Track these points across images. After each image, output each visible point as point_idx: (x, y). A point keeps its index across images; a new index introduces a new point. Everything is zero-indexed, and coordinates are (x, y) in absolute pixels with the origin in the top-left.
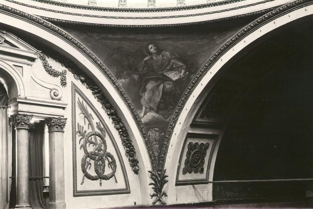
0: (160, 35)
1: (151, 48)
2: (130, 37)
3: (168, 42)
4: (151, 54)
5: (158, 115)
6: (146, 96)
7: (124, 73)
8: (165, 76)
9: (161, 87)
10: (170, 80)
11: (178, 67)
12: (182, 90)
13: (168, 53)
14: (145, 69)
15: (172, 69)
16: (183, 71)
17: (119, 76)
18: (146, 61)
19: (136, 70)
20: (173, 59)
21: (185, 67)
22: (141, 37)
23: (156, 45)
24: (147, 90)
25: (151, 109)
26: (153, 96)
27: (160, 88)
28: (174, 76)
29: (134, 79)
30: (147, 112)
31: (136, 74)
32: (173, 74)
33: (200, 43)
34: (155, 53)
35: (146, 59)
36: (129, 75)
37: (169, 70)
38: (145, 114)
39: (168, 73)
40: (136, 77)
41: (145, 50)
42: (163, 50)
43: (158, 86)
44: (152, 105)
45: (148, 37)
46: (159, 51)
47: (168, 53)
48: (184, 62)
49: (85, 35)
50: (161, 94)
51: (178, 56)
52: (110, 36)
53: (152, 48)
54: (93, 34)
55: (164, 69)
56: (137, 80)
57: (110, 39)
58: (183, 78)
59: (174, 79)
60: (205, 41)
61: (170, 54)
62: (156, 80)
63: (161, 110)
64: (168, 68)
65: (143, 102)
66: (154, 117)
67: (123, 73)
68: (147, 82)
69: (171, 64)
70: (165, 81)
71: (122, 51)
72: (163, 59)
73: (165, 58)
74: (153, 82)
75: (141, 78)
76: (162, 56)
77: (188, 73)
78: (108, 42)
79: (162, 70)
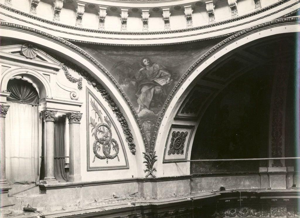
0: (151, 52)
1: (145, 61)
2: (129, 53)
3: (158, 57)
4: (145, 66)
5: (150, 111)
6: (141, 97)
7: (125, 80)
9: (152, 90)
10: (159, 85)
11: (165, 76)
12: (168, 93)
13: (157, 66)
15: (160, 77)
16: (169, 79)
17: (121, 82)
18: (141, 71)
19: (134, 78)
20: (161, 69)
21: (170, 76)
22: (137, 53)
24: (142, 93)
25: (145, 107)
26: (146, 97)
30: (142, 109)
33: (181, 58)
34: (148, 65)
35: (141, 69)
36: (129, 81)
37: (158, 78)
38: (140, 110)
39: (158, 80)
41: (140, 63)
42: (154, 63)
43: (150, 90)
44: (145, 104)
45: (142, 53)
46: (151, 64)
47: (157, 66)
48: (170, 72)
49: (96, 52)
50: (152, 95)
51: (165, 68)
52: (115, 53)
53: (146, 62)
54: (102, 51)
56: (134, 85)
58: (169, 84)
59: (162, 84)
60: (186, 56)
61: (159, 66)
62: (149, 85)
63: (152, 107)
64: (158, 76)
65: (139, 101)
66: (147, 113)
67: (124, 80)
68: (142, 86)
69: (160, 73)
70: (156, 86)
71: (123, 64)
72: (154, 70)
73: (155, 69)
75: (137, 83)
76: (153, 68)
77: (172, 80)
78: (113, 57)
79: (154, 78)
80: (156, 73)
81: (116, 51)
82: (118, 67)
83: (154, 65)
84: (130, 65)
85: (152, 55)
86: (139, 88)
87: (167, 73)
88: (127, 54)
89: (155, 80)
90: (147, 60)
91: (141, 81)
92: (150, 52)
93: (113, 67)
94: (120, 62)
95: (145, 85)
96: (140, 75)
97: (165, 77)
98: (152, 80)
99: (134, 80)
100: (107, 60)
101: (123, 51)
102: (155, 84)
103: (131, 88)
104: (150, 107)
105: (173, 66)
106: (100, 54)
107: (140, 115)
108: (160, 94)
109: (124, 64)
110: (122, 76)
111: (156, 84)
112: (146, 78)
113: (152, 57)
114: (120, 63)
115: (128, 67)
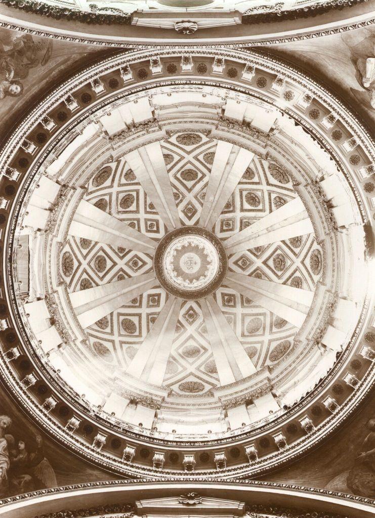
0: (19, 107)
1: (17, 88)
2: (45, 81)
3: (7, 108)
4: (12, 83)
7: (22, 43)
17: (28, 38)
18: (10, 72)
19: (12, 56)
22: (35, 90)
23: (15, 95)
29: (8, 44)
31: (9, 51)
34: (9, 87)
35: (12, 74)
36: (16, 45)
40: (7, 48)
41: (21, 81)
42: (4, 97)
45: (28, 96)
52: (62, 67)
53: (16, 89)
54: (81, 57)
56: (4, 46)
67: (24, 42)
71: (41, 61)
78: (60, 59)
81: (62, 70)
82: (44, 52)
84: (32, 67)
85: (16, 104)
88: (45, 79)
90: (15, 93)
92: (21, 105)
94: (46, 61)
96: (7, 66)
99: (10, 53)
100: (66, 51)
101: (55, 77)
106: (81, 51)
110: (31, 44)
113: (12, 102)
114: (46, 60)
115: (33, 63)
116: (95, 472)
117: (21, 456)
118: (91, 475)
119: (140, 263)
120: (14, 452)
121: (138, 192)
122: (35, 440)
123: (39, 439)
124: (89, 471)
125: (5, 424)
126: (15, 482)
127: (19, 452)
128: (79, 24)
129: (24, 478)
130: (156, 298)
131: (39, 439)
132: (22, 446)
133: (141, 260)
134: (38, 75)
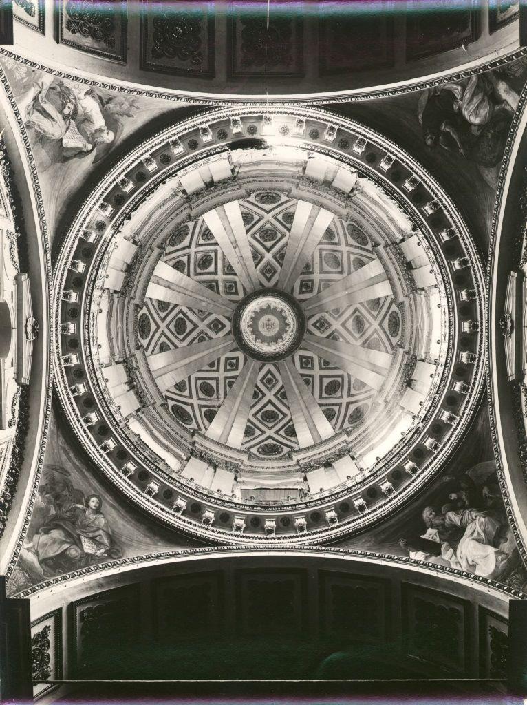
1: (93, 501)
2: (86, 473)
3: (113, 511)
4: (88, 506)
5: (39, 565)
6: (43, 538)
7: (47, 496)
8: (79, 540)
9: (66, 546)
10: (82, 548)
12: (87, 564)
13: (103, 521)
14: (68, 514)
15: (93, 539)
16: (103, 551)
17: (42, 490)
18: (76, 508)
19: (60, 506)
21: (107, 548)
22: (94, 483)
23: (100, 503)
25: (37, 553)
27: (63, 546)
28: (88, 547)
29: (48, 510)
31: (55, 509)
32: (89, 545)
33: (141, 538)
34: (92, 509)
36: (50, 502)
38: (28, 549)
40: (53, 511)
42: (101, 513)
43: (63, 542)
44: (40, 551)
46: (98, 511)
47: (103, 521)
49: (55, 431)
50: (59, 552)
52: (72, 455)
53: (93, 502)
55: (84, 532)
57: (70, 459)
59: (86, 551)
61: (105, 523)
62: (68, 535)
63: (46, 564)
64: (90, 534)
65: (36, 537)
66: (33, 563)
67: (47, 493)
68: (57, 527)
69: (97, 533)
70: (77, 545)
72: (93, 522)
73: (97, 522)
74: (63, 534)
75: (56, 517)
76: (96, 519)
78: (64, 457)
80: (92, 529)
81: (74, 455)
82: (56, 474)
83: (100, 516)
84: (72, 486)
86: (52, 525)
87: (106, 541)
89: (82, 537)
90: (97, 503)
91: (63, 519)
93: (52, 466)
95: (64, 529)
96: (70, 511)
97: (99, 544)
98: (78, 532)
99: (57, 508)
102: (77, 541)
103: (41, 512)
104: (43, 562)
105: (123, 539)
106: (55, 436)
107: (23, 552)
108: (73, 559)
109: (66, 479)
110: (49, 486)
111: (77, 542)
112: (74, 523)
113: (106, 505)
114: (64, 471)
115: (67, 484)
116: (480, 422)
117: (464, 497)
118: (483, 426)
119: (269, 376)
120: (459, 504)
121: (197, 379)
122: (448, 483)
123: (446, 479)
124: (479, 427)
125: (431, 514)
126: (490, 503)
127: (459, 499)
128: (28, 438)
129: (486, 494)
130: (304, 360)
131: (446, 479)
132: (454, 496)
133: (266, 375)
134: (78, 479)
